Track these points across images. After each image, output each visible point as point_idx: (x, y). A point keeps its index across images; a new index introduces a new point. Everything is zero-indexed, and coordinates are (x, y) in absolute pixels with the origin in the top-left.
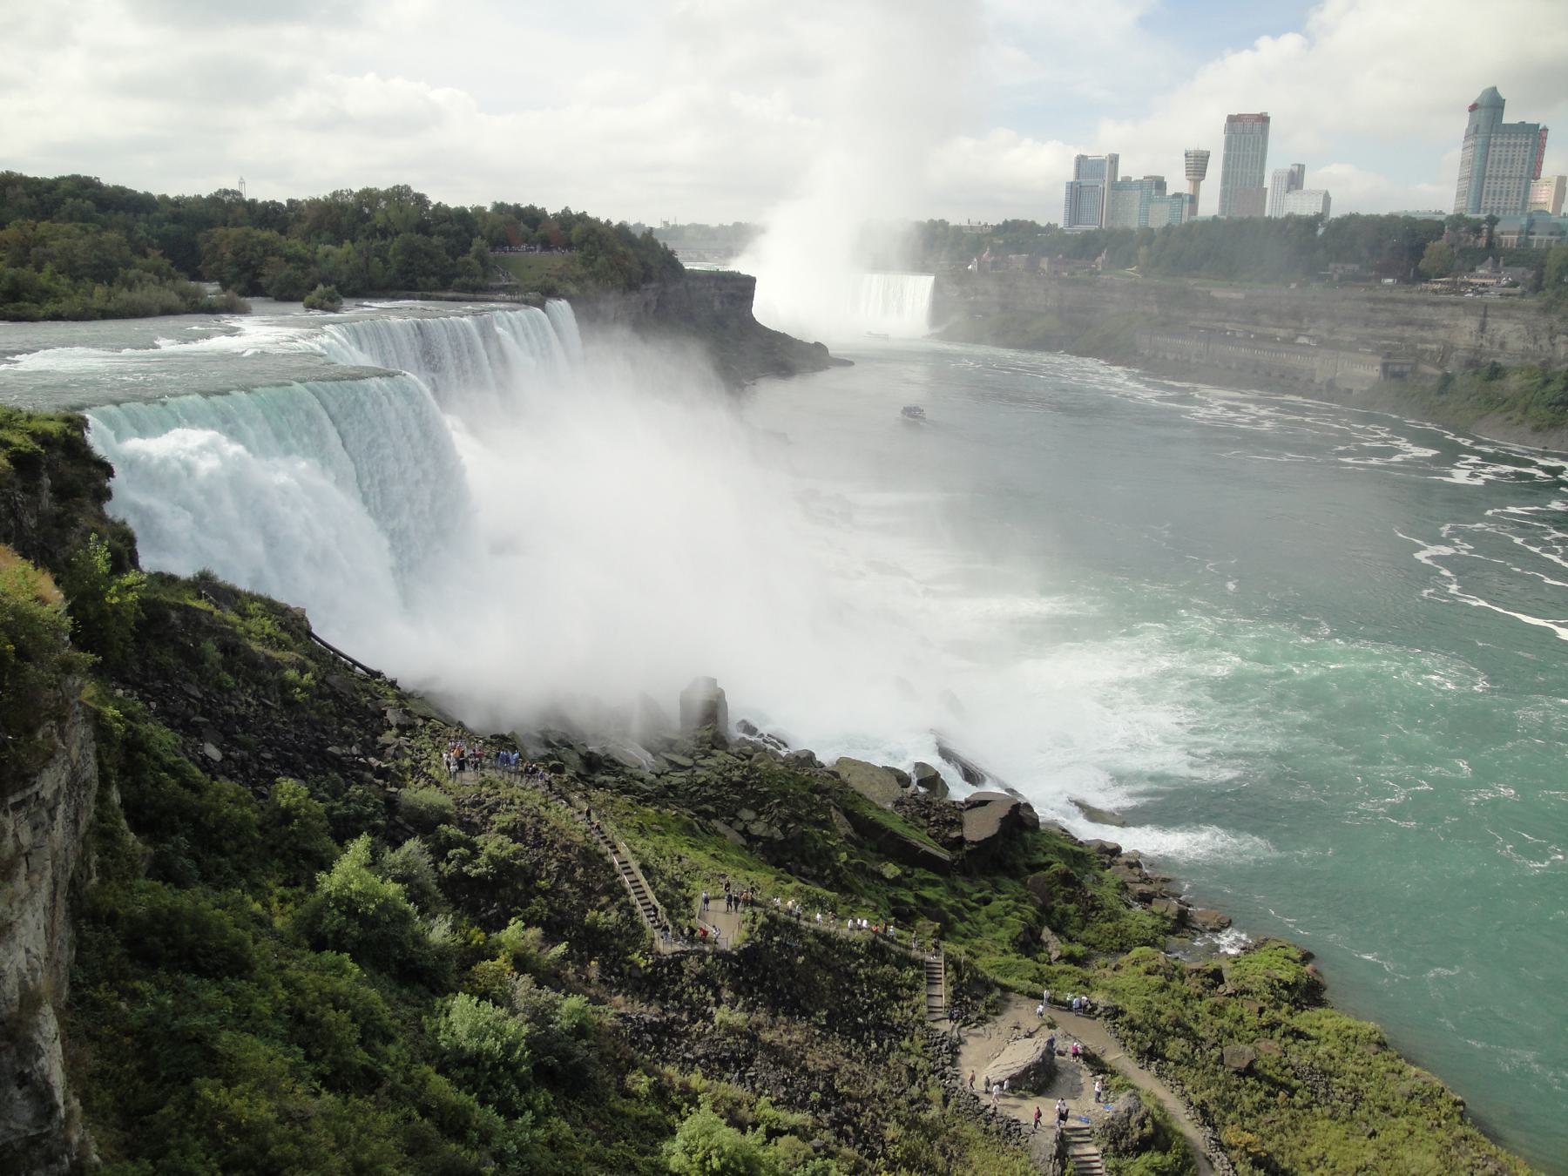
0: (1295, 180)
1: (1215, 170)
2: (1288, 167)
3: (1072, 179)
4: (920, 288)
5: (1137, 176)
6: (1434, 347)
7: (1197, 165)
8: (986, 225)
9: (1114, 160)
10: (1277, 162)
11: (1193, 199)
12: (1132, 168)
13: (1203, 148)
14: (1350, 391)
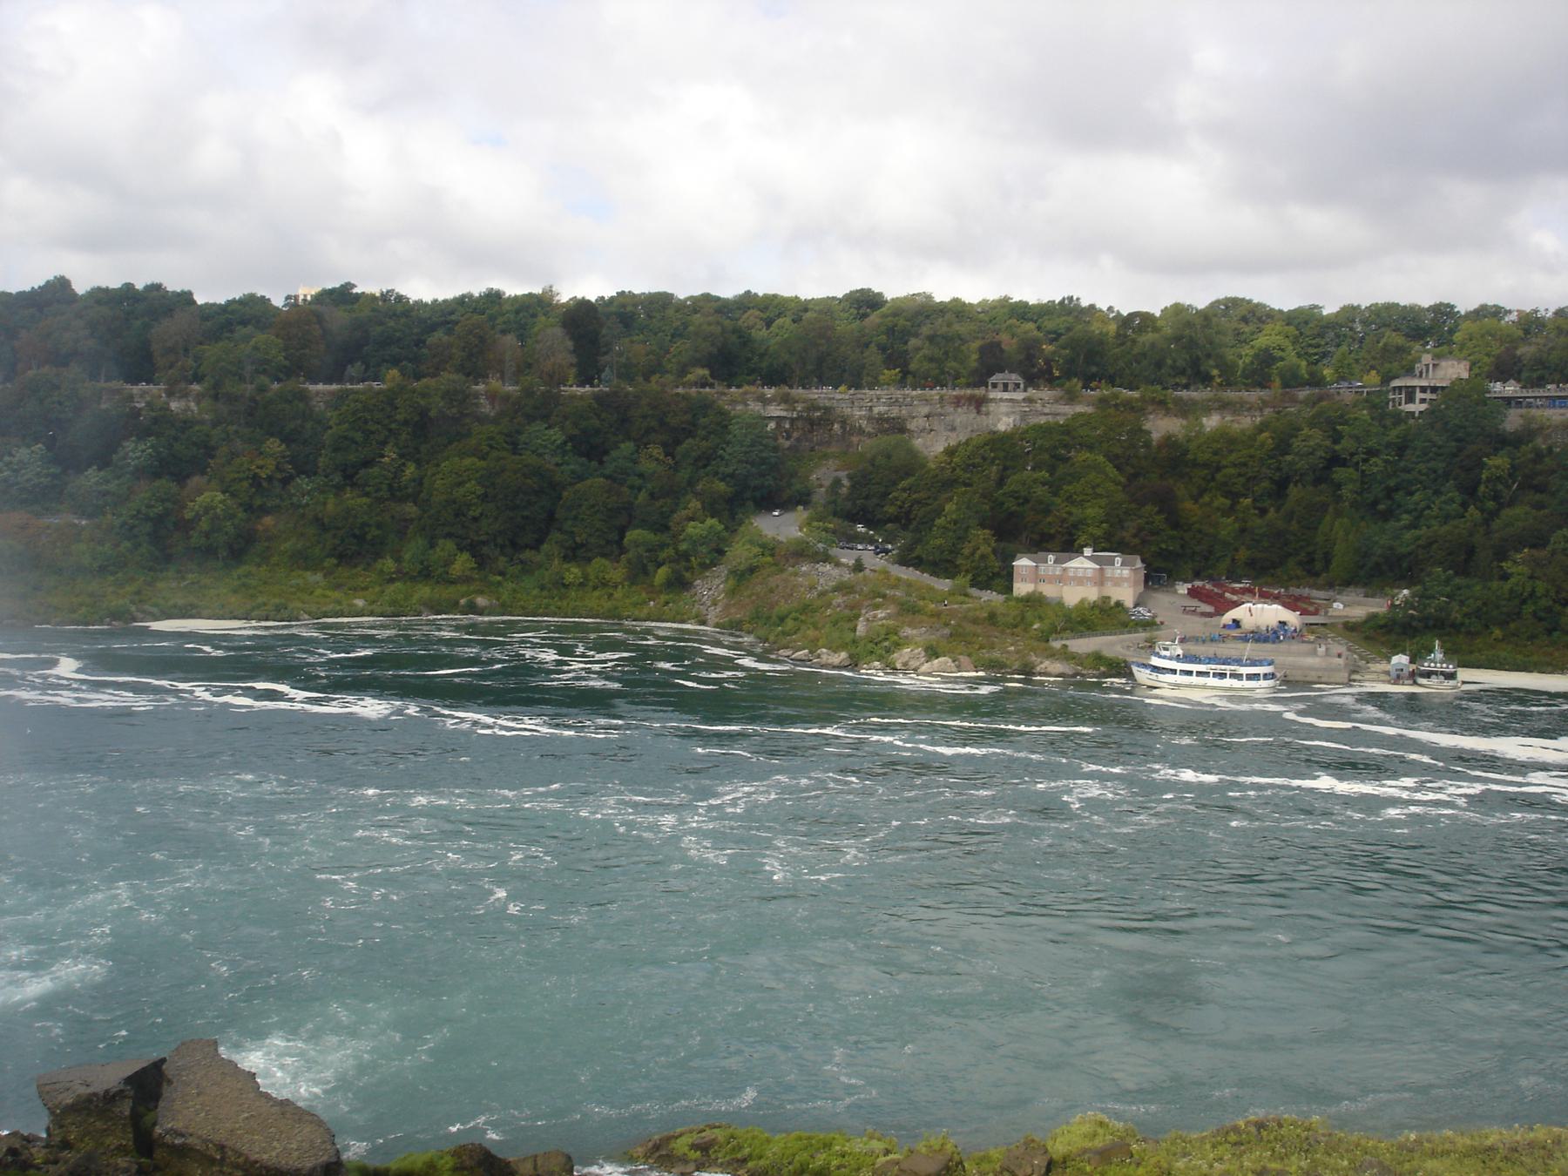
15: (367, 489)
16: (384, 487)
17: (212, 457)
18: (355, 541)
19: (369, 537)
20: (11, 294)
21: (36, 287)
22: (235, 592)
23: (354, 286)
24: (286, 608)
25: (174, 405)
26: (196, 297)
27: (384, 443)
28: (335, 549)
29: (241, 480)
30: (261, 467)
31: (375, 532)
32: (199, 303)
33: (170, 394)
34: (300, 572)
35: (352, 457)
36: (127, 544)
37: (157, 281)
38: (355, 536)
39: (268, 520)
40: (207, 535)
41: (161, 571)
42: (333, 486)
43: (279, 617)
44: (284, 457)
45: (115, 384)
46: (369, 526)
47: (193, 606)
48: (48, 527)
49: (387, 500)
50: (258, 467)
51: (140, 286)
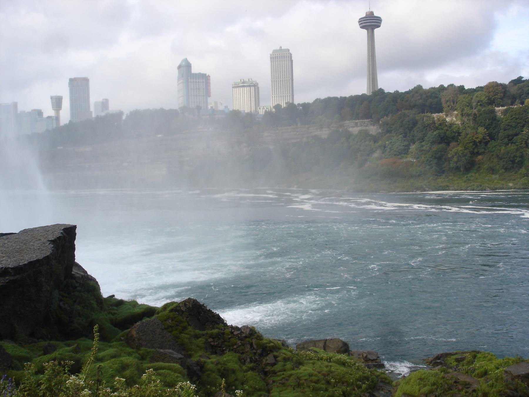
1: (66, 104)
2: (101, 100)
7: (57, 102)
10: (95, 97)
11: (57, 118)
13: (59, 94)
15: (517, 144)
16: (524, 142)
17: (460, 136)
18: (511, 163)
19: (516, 161)
20: (403, 93)
21: (411, 89)
22: (465, 182)
23: (522, 77)
24: (481, 186)
25: (448, 119)
26: (465, 87)
27: (523, 126)
28: (504, 166)
29: (470, 143)
30: (477, 138)
31: (518, 159)
32: (466, 89)
33: (447, 116)
34: (490, 175)
35: (511, 132)
36: (428, 167)
37: (451, 83)
38: (511, 161)
39: (480, 157)
40: (456, 162)
41: (440, 176)
42: (504, 144)
43: (478, 189)
44: (486, 134)
45: (429, 114)
46: (517, 157)
47: (448, 186)
48: (403, 163)
49: (524, 147)
50: (476, 138)
51: (446, 85)
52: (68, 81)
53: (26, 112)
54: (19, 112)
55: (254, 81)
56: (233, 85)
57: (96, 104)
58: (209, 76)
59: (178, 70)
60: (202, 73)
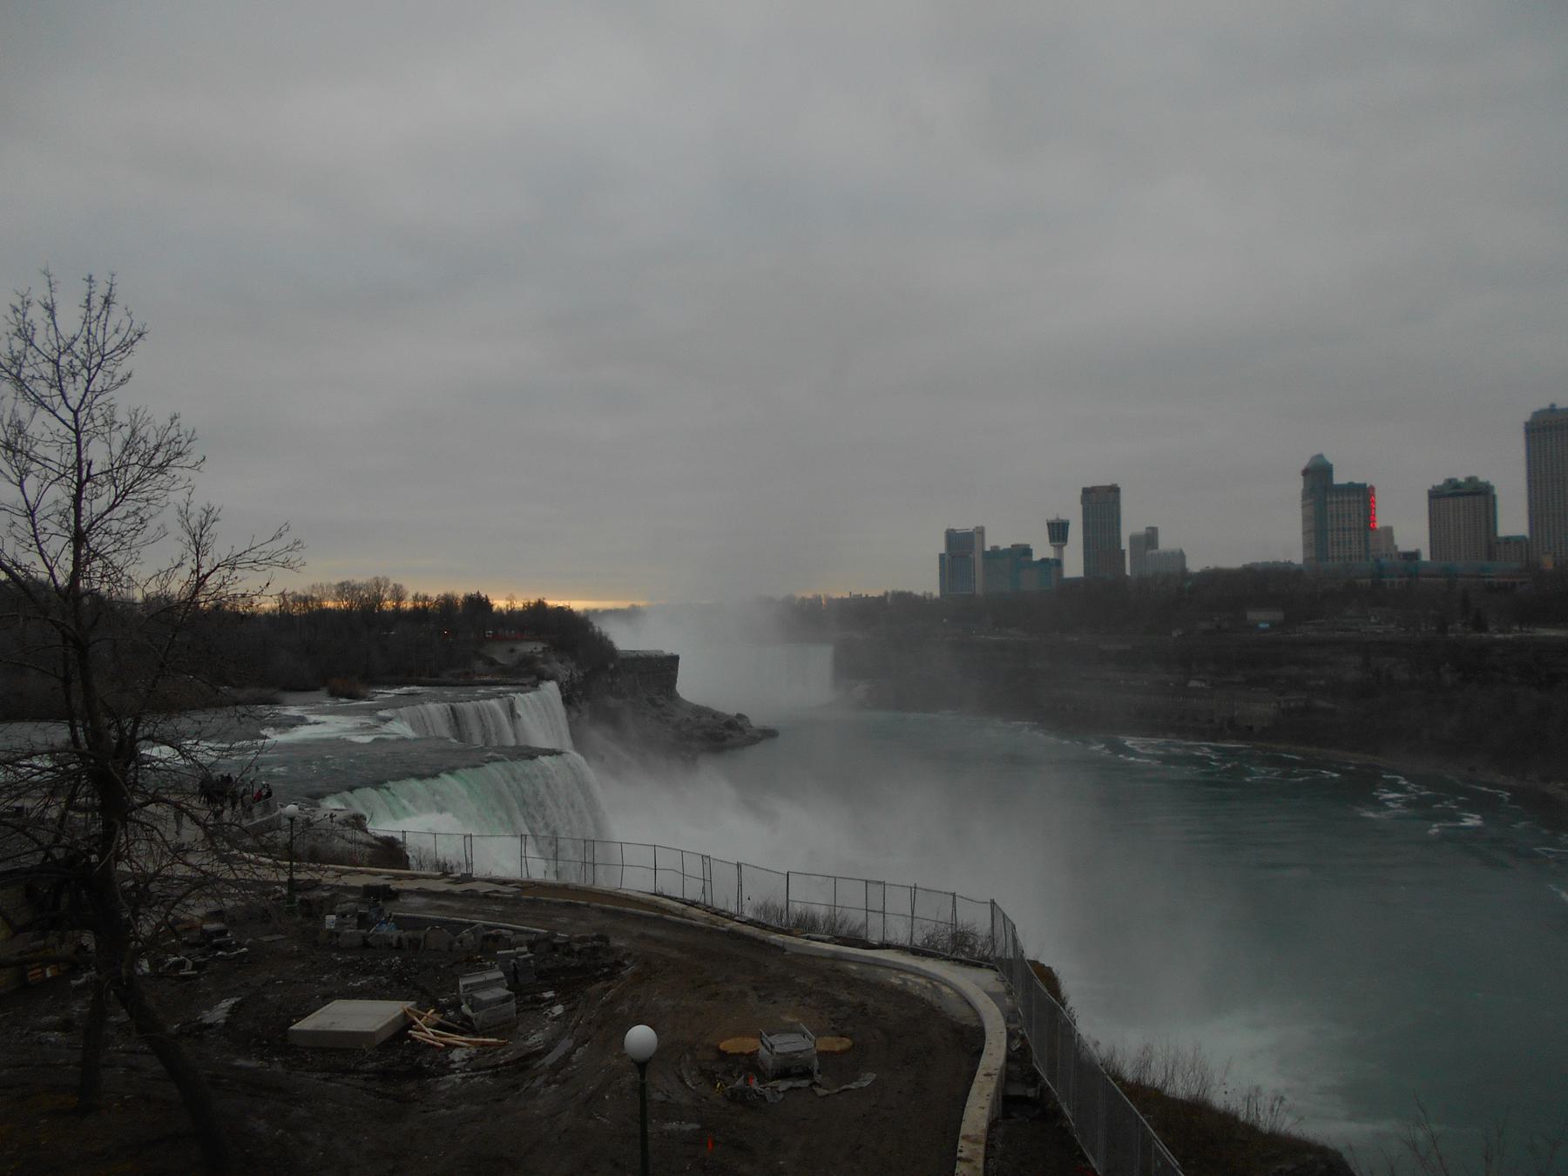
0: (1150, 537)
3: (943, 551)
4: (822, 657)
5: (1004, 544)
6: (1322, 682)
7: (1058, 532)
8: (867, 595)
9: (981, 531)
10: (1131, 523)
11: (1058, 563)
12: (999, 537)
13: (1063, 517)
14: (1251, 728)
52: (1080, 493)
53: (1001, 548)
54: (988, 548)
55: (1482, 483)
56: (1430, 492)
57: (1134, 540)
58: (1372, 488)
59: (1302, 477)
60: (1356, 482)
